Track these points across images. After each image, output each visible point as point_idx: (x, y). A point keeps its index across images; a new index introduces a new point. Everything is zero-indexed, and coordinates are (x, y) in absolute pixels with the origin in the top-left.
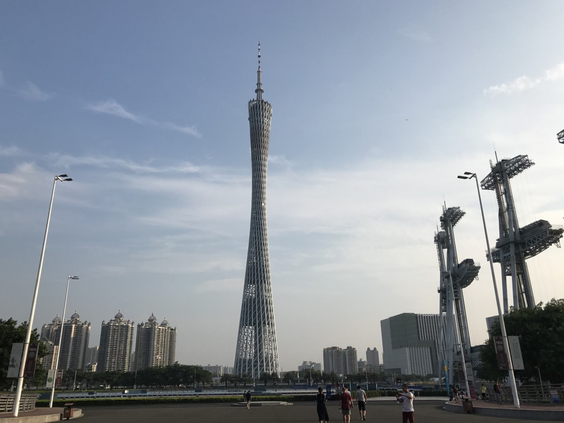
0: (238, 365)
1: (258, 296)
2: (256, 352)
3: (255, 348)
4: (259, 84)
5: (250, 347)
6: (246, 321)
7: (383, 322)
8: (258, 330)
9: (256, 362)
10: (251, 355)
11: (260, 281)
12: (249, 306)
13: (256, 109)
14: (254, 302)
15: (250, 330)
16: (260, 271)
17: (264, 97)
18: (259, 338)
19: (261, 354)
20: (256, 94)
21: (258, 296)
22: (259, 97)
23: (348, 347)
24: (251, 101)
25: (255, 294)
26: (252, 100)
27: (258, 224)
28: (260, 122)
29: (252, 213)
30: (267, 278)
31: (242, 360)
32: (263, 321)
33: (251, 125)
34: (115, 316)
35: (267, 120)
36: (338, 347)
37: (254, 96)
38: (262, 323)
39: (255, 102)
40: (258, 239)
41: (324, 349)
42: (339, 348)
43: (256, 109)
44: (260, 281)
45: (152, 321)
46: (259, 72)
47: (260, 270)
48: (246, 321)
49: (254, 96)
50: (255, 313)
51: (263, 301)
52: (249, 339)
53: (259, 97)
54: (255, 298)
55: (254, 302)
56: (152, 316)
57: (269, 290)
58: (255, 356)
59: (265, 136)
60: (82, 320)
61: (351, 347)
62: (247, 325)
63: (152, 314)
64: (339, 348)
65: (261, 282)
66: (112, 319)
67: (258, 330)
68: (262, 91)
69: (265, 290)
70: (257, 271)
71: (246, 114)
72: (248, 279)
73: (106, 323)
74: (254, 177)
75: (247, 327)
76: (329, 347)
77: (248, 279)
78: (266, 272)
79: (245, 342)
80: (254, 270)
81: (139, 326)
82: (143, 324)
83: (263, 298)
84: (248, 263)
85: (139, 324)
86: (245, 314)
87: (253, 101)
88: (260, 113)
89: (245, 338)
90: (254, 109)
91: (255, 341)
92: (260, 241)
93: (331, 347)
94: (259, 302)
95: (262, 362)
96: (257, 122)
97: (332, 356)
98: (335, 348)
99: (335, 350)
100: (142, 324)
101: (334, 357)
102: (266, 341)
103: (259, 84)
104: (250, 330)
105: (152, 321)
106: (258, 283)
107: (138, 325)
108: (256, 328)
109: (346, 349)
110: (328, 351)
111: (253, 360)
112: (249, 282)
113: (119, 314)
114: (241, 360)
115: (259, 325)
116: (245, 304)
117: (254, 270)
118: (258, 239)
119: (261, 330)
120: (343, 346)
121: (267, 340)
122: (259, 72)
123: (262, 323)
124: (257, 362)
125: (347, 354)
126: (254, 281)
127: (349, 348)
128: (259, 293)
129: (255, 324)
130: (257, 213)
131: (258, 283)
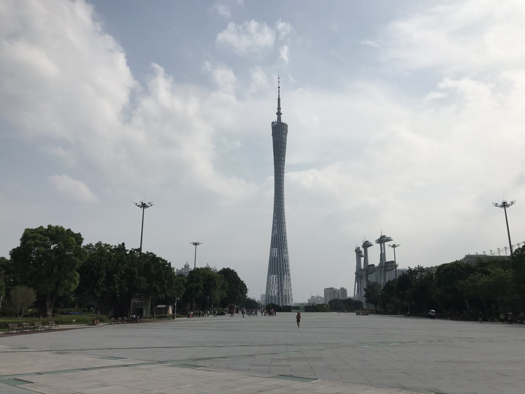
0: (267, 300)
1: (280, 257)
2: (279, 292)
3: (278, 289)
4: (279, 108)
5: (275, 283)
6: (272, 272)
8: (279, 278)
9: (279, 298)
10: (276, 288)
11: (280, 247)
12: (274, 267)
13: (277, 128)
14: (277, 260)
15: (274, 277)
16: (281, 241)
17: (283, 120)
18: (281, 283)
19: (282, 293)
20: (277, 115)
21: (280, 257)
22: (279, 118)
25: (277, 255)
26: (275, 122)
27: (279, 209)
28: (280, 138)
29: (275, 202)
30: (285, 245)
31: (270, 296)
33: (271, 259)
38: (282, 274)
41: (325, 289)
42: (335, 288)
43: (277, 128)
47: (281, 239)
48: (272, 272)
49: (275, 119)
50: (278, 263)
51: (283, 260)
52: (274, 278)
53: (279, 118)
55: (277, 260)
57: (287, 253)
58: (278, 294)
62: (273, 275)
64: (335, 288)
65: (281, 247)
67: (279, 278)
68: (281, 114)
69: (284, 253)
70: (279, 240)
72: (273, 245)
74: (276, 176)
75: (272, 275)
77: (273, 245)
78: (285, 241)
79: (272, 280)
80: (277, 240)
83: (283, 259)
84: (272, 235)
86: (271, 268)
88: (280, 132)
89: (272, 278)
90: (275, 128)
91: (278, 285)
92: (278, 245)
93: (329, 288)
94: (280, 260)
95: (283, 298)
96: (278, 138)
97: (330, 294)
98: (332, 288)
99: (332, 290)
101: (331, 295)
102: (285, 285)
103: (279, 108)
104: (274, 277)
106: (279, 248)
108: (278, 277)
111: (277, 297)
112: (274, 247)
114: (269, 296)
115: (281, 275)
116: (271, 266)
117: (277, 240)
119: (282, 279)
120: (339, 288)
121: (286, 284)
123: (282, 274)
124: (280, 298)
125: (340, 292)
126: (277, 246)
127: (342, 289)
128: (280, 255)
130: (279, 205)
131: (279, 248)
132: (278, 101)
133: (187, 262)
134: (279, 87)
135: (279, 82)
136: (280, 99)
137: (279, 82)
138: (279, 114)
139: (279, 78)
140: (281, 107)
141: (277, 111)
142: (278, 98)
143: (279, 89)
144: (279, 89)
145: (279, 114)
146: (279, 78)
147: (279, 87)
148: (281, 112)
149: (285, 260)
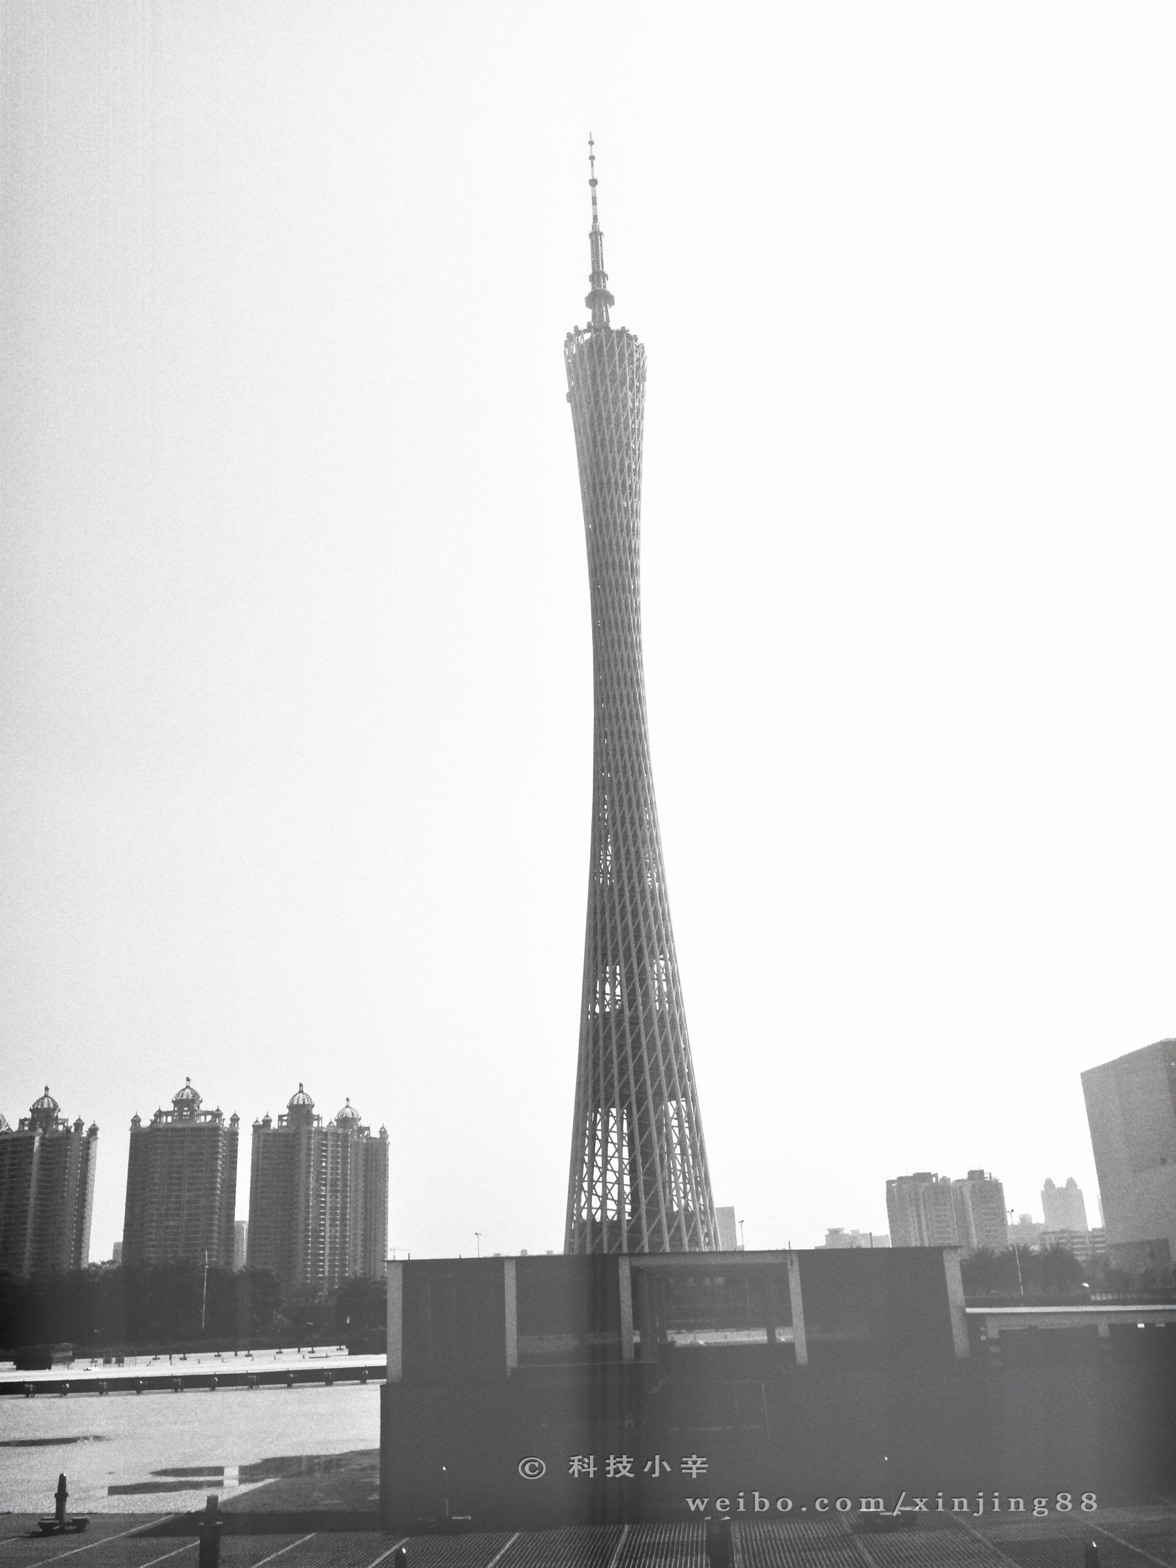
4: (598, 276)
7: (1088, 1078)
14: (620, 1023)
23: (972, 1174)
24: (569, 335)
32: (652, 1086)
34: (172, 1097)
35: (630, 394)
36: (936, 1175)
37: (585, 317)
39: (587, 336)
40: (621, 806)
42: (940, 1177)
44: (634, 952)
45: (300, 1112)
46: (596, 236)
54: (621, 1011)
56: (301, 1091)
59: (624, 448)
60: (68, 1114)
61: (982, 1172)
63: (301, 1085)
64: (940, 1177)
66: (163, 1110)
71: (559, 383)
73: (145, 1123)
76: (904, 1174)
81: (256, 1128)
82: (271, 1121)
85: (257, 1121)
87: (578, 332)
93: (911, 1174)
98: (923, 1177)
99: (923, 1185)
100: (267, 1122)
103: (598, 276)
105: (300, 1112)
107: (253, 1126)
109: (965, 1180)
110: (899, 1187)
113: (188, 1091)
118: (621, 806)
120: (954, 1171)
122: (596, 236)
125: (967, 1193)
126: (615, 949)
127: (976, 1176)
129: (624, 1098)
132: (592, 241)
133: (188, 1080)
134: (593, 182)
135: (592, 158)
136: (601, 234)
137: (592, 158)
138: (599, 299)
139: (591, 143)
140: (606, 270)
141: (587, 288)
142: (590, 229)
143: (594, 192)
144: (594, 192)
145: (599, 299)
146: (591, 143)
147: (593, 182)
148: (610, 286)
149: (662, 1019)
